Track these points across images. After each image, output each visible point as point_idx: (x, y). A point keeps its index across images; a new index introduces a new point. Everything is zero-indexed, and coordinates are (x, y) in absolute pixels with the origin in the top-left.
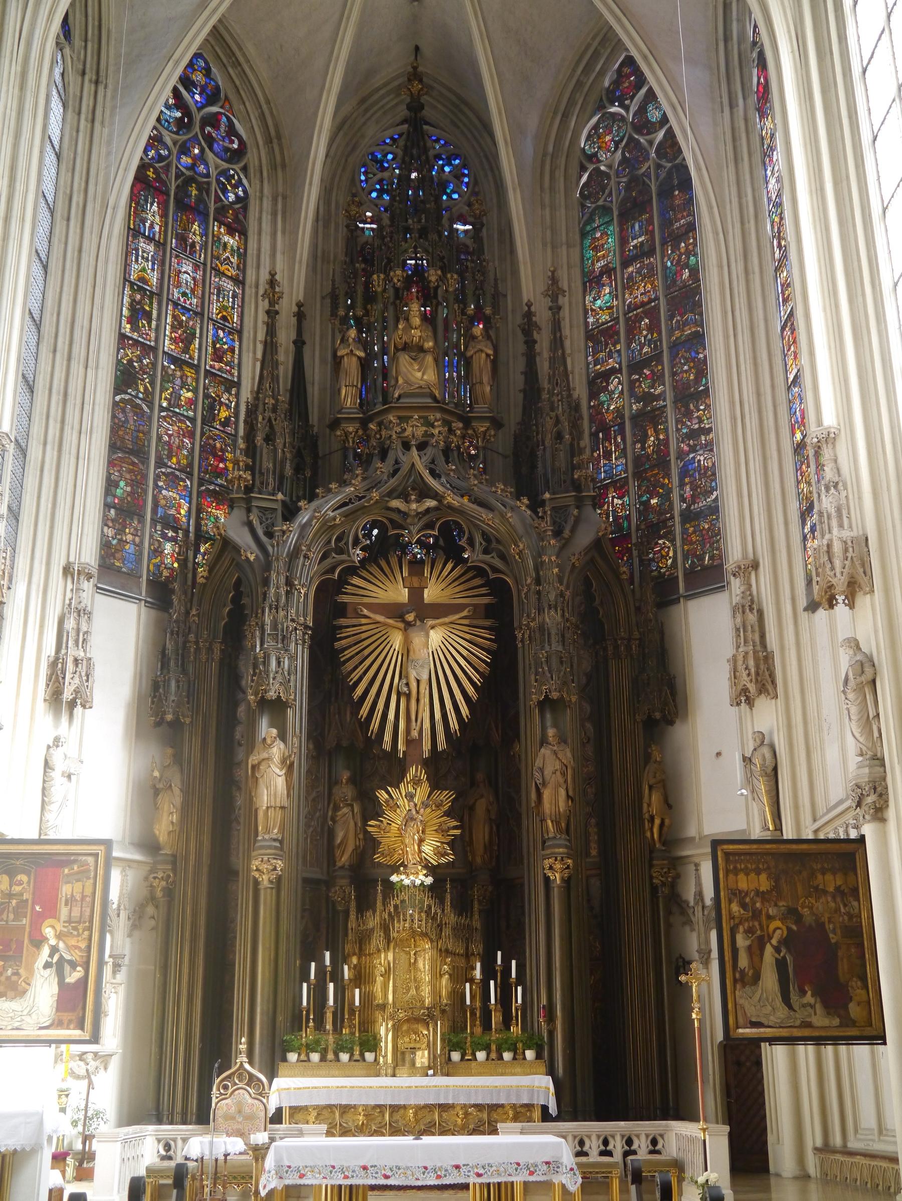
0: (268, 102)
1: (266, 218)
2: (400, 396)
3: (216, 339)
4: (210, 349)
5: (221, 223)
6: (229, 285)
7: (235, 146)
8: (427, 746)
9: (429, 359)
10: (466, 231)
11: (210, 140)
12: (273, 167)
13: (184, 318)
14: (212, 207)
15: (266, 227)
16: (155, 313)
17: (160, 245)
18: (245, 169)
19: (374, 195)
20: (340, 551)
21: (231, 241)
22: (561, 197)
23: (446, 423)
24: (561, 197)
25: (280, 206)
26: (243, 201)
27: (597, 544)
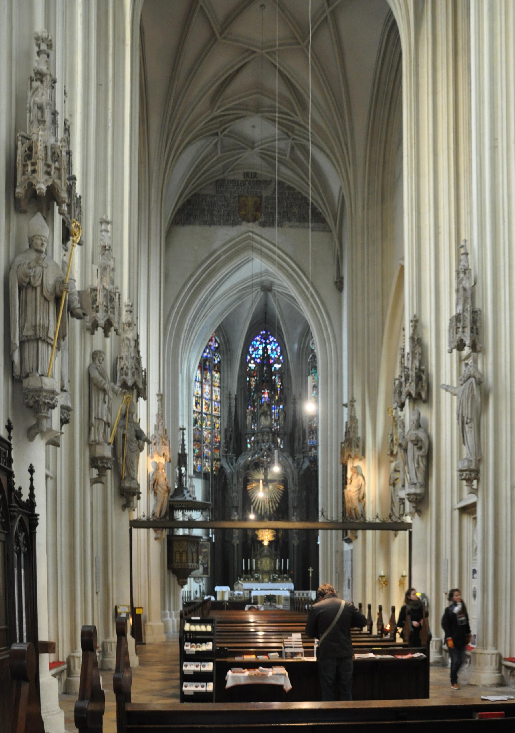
0: (225, 331)
1: (225, 367)
2: (262, 428)
3: (215, 405)
4: (213, 409)
5: (214, 371)
6: (217, 389)
7: (217, 345)
8: (268, 513)
9: (269, 418)
10: (279, 368)
11: (210, 346)
12: (227, 350)
13: (207, 402)
14: (212, 365)
15: (225, 369)
16: (200, 402)
17: (201, 383)
18: (219, 352)
19: (253, 356)
20: (248, 469)
21: (217, 375)
22: (304, 361)
23: (273, 436)
24: (304, 361)
25: (229, 364)
26: (219, 362)
27: (308, 468)
